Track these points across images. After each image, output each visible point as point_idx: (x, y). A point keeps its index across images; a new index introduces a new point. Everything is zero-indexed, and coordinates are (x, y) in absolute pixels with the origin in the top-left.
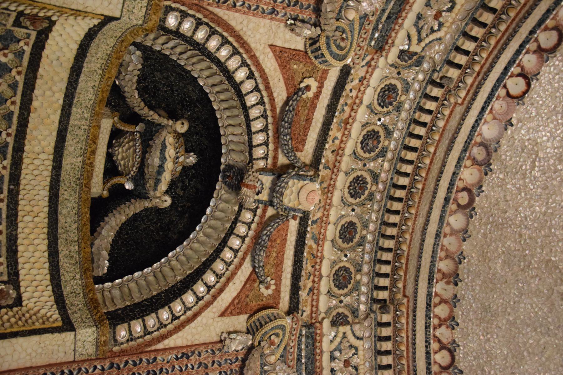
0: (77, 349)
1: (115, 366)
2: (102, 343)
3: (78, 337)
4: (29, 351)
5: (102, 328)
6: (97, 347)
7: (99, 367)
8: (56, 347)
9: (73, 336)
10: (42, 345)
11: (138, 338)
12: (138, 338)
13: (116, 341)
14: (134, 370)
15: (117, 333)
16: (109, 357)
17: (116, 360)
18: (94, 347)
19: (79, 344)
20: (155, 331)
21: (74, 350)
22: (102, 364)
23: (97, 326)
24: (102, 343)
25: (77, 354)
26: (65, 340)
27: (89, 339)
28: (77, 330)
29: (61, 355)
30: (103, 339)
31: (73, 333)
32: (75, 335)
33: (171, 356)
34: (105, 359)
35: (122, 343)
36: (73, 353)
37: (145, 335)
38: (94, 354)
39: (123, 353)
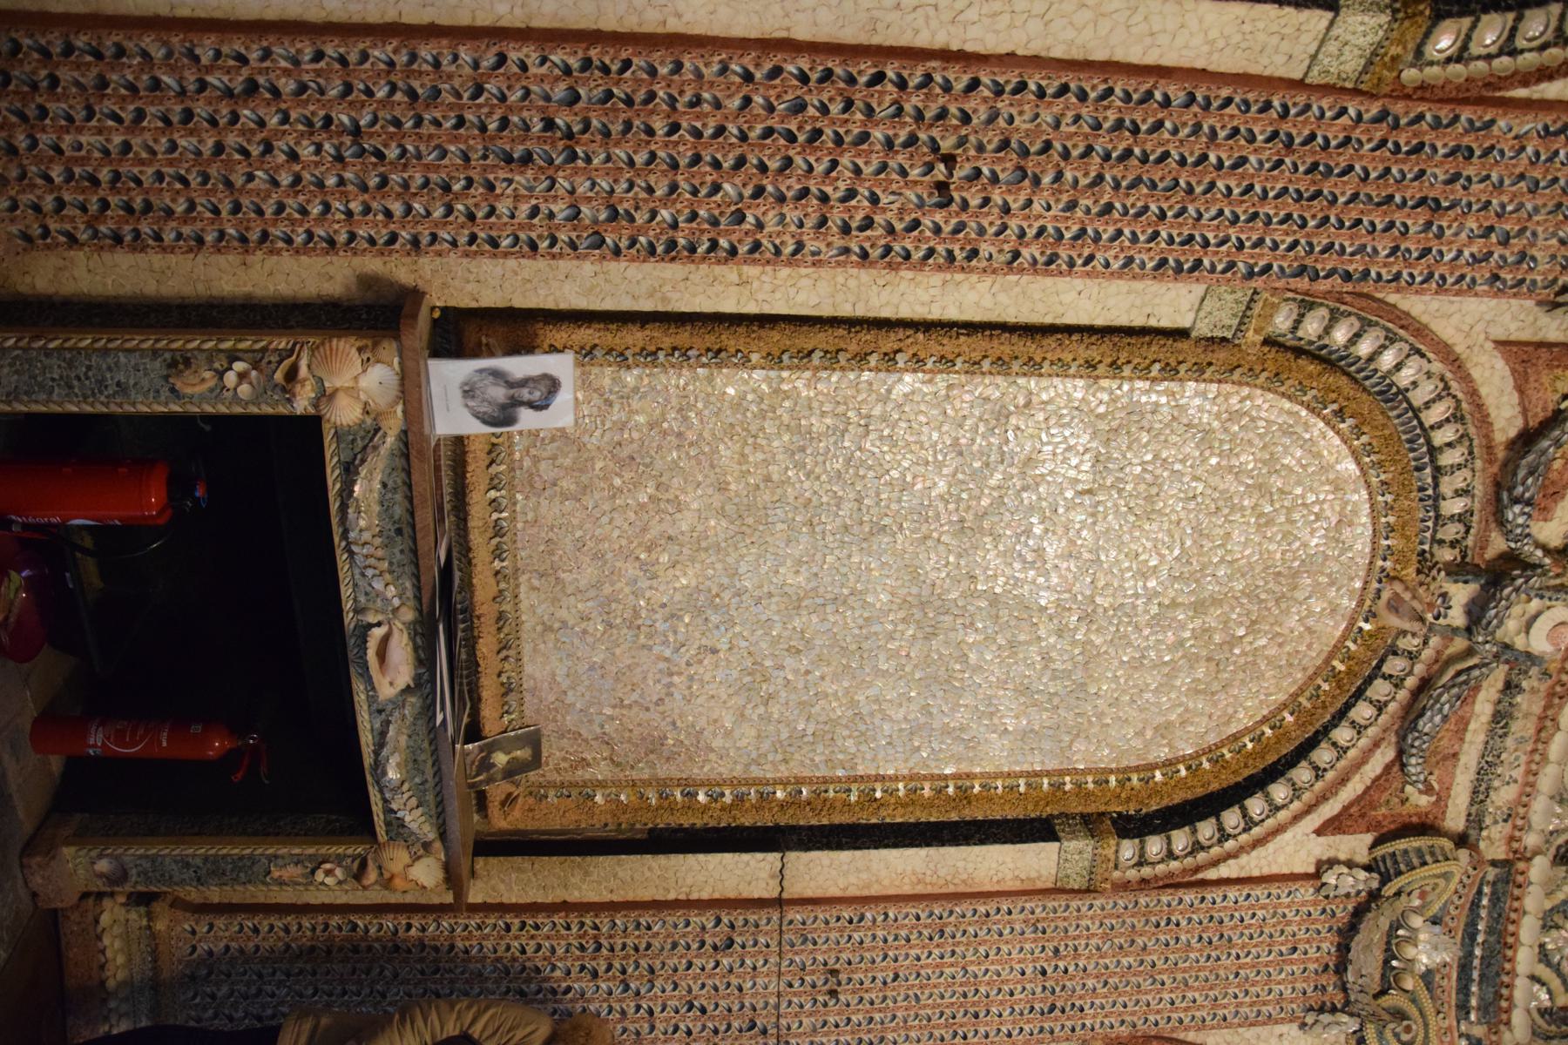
0: (1320, 56)
1: (1390, 119)
2: (1387, 59)
3: (1335, 32)
4: (1214, 34)
5: (1407, 24)
6: (1370, 63)
7: (1352, 112)
8: (1275, 40)
9: (1324, 23)
10: (1247, 28)
11: (1479, 58)
12: (1479, 58)
13: (1419, 53)
14: (1427, 139)
15: (1433, 37)
16: (1385, 96)
17: (1398, 108)
18: (1363, 61)
19: (1332, 47)
20: (1530, 50)
21: (1314, 57)
22: (1362, 109)
23: (1395, 11)
24: (1387, 59)
25: (1315, 71)
26: (1303, 28)
27: (1361, 41)
28: (1343, 11)
29: (1280, 59)
30: (1395, 50)
31: (1330, 15)
32: (1332, 23)
33: (1528, 124)
34: (1372, 96)
35: (1431, 63)
36: (1307, 62)
37: (1500, 54)
38: (1354, 76)
39: (1424, 91)
